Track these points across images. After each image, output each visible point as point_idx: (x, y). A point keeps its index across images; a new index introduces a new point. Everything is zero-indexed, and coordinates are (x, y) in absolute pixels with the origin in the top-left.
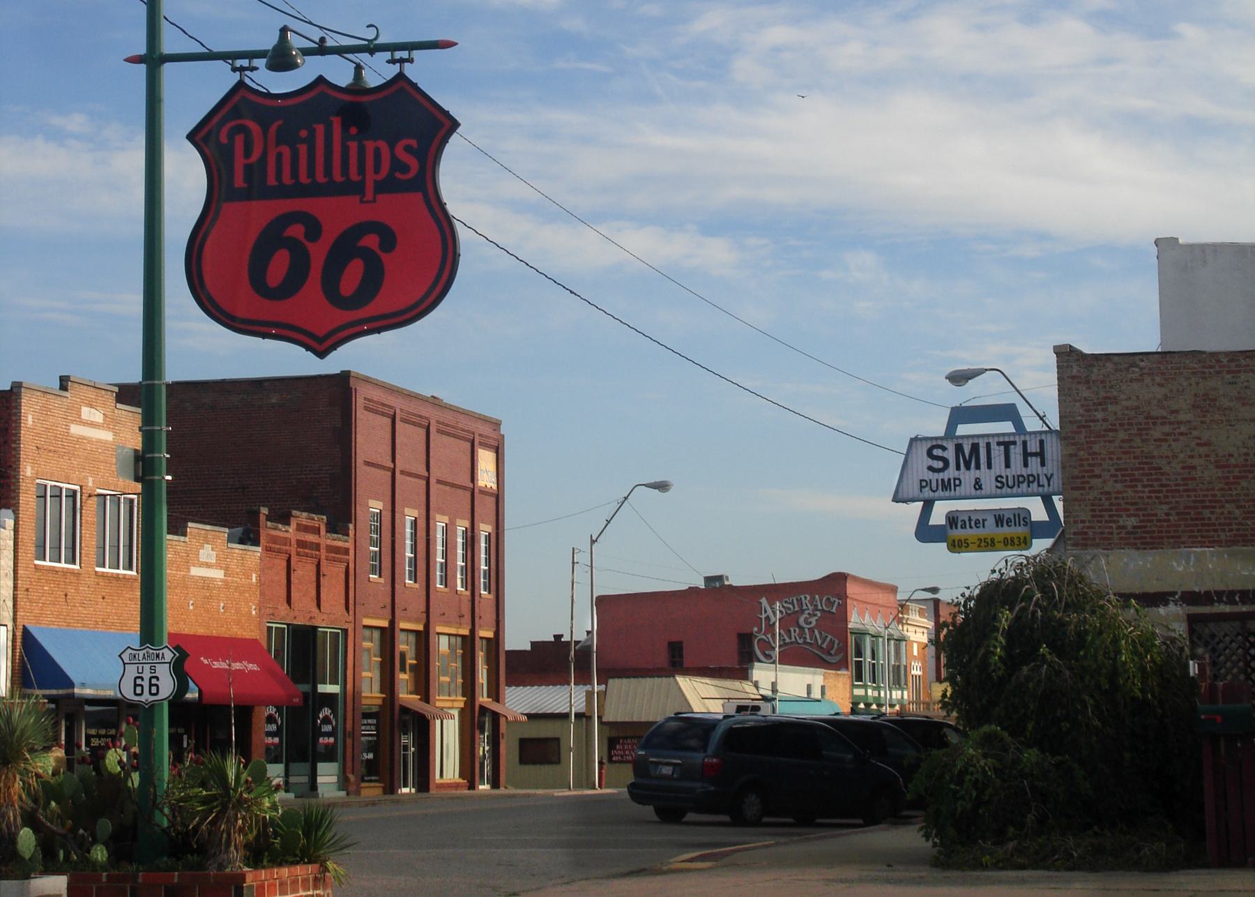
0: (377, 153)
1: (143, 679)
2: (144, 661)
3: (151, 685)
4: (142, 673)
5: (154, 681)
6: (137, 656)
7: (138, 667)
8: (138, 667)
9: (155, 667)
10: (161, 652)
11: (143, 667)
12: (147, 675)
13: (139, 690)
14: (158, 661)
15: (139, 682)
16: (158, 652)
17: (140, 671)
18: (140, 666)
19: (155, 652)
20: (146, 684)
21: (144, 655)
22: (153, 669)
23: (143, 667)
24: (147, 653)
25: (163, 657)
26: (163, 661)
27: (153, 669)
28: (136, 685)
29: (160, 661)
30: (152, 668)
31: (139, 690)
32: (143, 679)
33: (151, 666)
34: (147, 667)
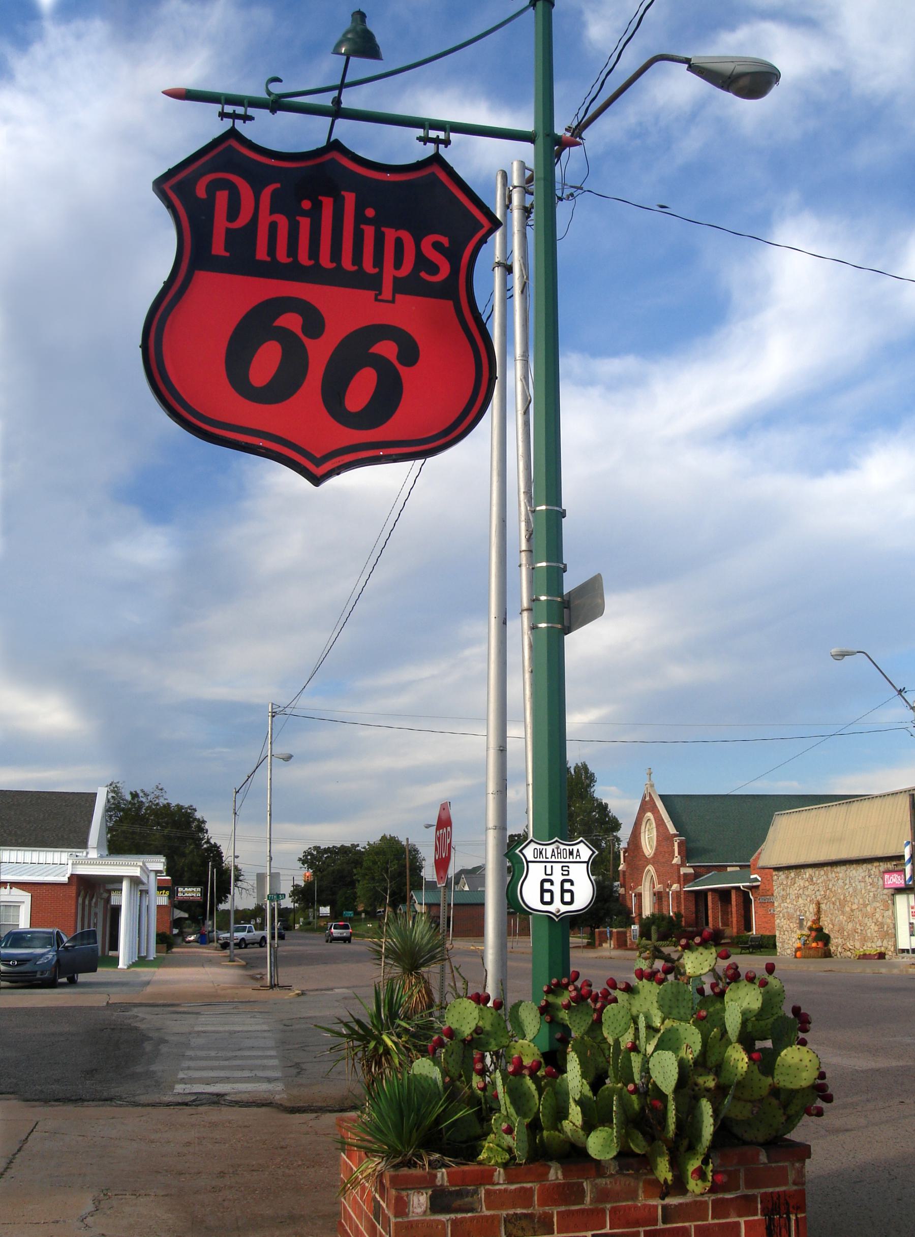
0: (399, 243)
1: (552, 884)
2: (553, 859)
3: (563, 891)
4: (551, 875)
5: (567, 886)
6: (544, 852)
7: (545, 866)
8: (545, 866)
9: (568, 867)
10: (575, 848)
11: (552, 866)
12: (557, 878)
13: (547, 897)
14: (571, 860)
15: (547, 886)
16: (571, 848)
17: (549, 872)
18: (549, 865)
19: (567, 848)
20: (557, 889)
21: (553, 851)
22: (565, 871)
23: (552, 866)
24: (558, 848)
25: (578, 855)
26: (578, 860)
27: (565, 871)
28: (543, 891)
29: (575, 860)
30: (564, 868)
31: (547, 897)
32: (552, 883)
33: (563, 867)
34: (557, 867)
